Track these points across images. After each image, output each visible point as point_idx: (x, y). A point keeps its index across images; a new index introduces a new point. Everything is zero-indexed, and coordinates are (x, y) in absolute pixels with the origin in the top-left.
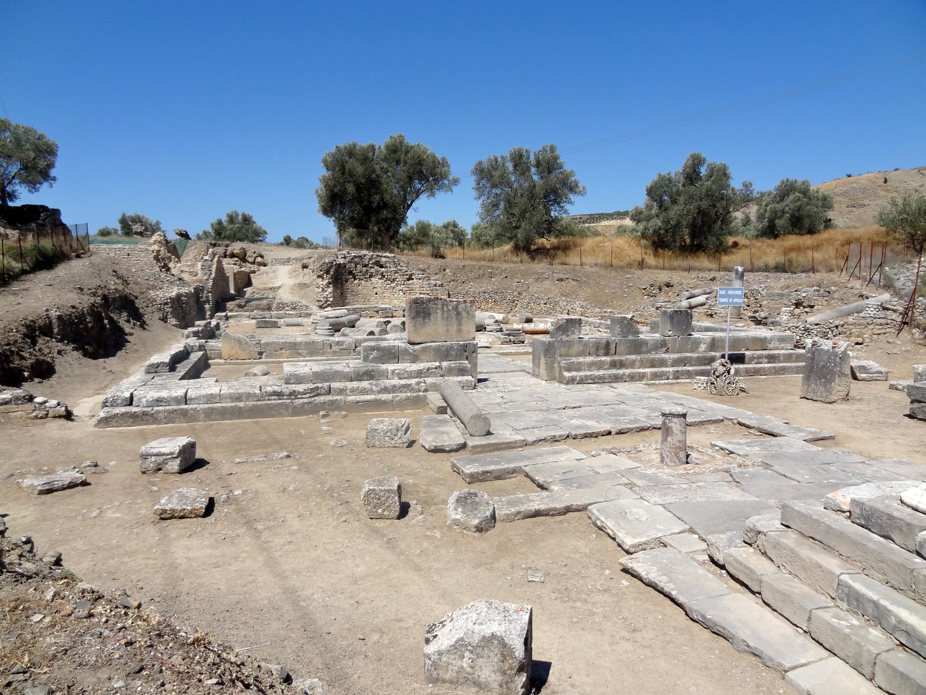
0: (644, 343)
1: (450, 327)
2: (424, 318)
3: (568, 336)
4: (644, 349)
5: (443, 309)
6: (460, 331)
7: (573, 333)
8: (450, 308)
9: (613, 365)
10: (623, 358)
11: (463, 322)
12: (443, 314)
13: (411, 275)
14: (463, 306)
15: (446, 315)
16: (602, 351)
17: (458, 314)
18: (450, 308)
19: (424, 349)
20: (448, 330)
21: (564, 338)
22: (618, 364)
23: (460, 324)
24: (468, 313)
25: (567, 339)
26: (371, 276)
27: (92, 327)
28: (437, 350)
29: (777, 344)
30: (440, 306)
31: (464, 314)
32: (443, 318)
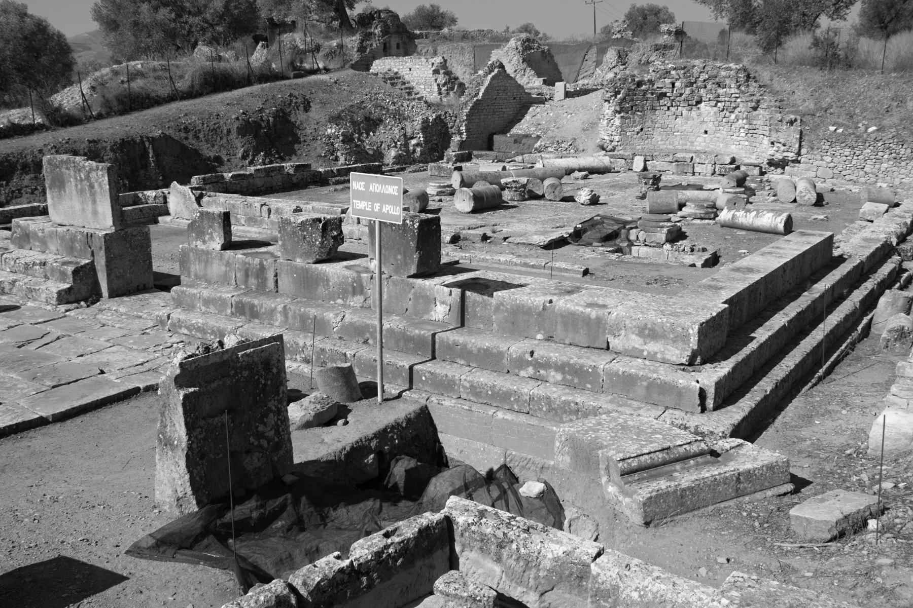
0: (325, 279)
3: (204, 242)
4: (321, 290)
6: (95, 213)
7: (212, 239)
8: (83, 176)
12: (76, 186)
13: (758, 101)
15: (79, 186)
17: (91, 187)
18: (83, 176)
20: (83, 210)
23: (94, 202)
24: (100, 185)
25: (203, 247)
26: (698, 102)
28: (62, 239)
29: (635, 341)
30: (72, 173)
31: (96, 185)
32: (77, 190)
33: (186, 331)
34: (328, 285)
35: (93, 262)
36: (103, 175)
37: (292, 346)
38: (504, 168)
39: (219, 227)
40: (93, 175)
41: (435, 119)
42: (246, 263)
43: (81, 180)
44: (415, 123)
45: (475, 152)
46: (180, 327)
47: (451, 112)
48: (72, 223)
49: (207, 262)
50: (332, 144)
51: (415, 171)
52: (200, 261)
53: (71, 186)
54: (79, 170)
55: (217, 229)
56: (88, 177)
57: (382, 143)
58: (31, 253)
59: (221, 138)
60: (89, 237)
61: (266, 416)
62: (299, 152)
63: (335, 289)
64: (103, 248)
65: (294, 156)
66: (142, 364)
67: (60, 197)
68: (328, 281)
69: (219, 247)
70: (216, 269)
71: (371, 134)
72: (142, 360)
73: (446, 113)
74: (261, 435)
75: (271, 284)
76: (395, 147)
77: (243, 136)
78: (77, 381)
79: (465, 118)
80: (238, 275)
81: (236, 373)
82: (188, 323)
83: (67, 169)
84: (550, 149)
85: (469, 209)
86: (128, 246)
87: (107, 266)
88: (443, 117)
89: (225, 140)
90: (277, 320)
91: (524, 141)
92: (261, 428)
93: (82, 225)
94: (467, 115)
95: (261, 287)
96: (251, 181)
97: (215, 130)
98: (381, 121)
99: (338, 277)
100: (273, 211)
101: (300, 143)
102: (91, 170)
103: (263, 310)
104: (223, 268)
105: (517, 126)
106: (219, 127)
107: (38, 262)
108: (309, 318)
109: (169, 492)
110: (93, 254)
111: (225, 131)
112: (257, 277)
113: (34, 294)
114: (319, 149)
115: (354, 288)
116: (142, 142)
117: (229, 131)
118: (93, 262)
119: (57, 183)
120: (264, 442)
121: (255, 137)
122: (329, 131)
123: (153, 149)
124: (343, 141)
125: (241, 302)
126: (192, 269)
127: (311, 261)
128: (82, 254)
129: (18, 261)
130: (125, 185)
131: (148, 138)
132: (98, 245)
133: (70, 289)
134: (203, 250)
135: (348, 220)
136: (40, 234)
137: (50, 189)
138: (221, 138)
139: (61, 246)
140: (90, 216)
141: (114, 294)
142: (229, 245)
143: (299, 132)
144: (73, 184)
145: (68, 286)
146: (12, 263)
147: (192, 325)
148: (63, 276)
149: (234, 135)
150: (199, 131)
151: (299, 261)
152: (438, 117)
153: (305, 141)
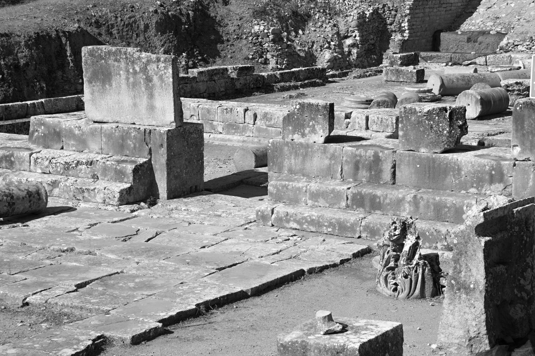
0: (458, 169)
1: (138, 100)
2: (104, 83)
3: (303, 135)
4: (451, 180)
5: (128, 71)
6: (151, 108)
9: (358, 201)
10: (379, 192)
11: (156, 93)
12: (127, 79)
14: (154, 66)
15: (131, 80)
16: (364, 174)
17: (149, 80)
18: (137, 69)
19: (93, 133)
20: (135, 105)
21: (297, 138)
22: (367, 203)
23: (151, 96)
24: (161, 78)
25: (302, 140)
27: (27, 65)
28: (109, 136)
30: (123, 65)
31: (155, 79)
32: (128, 84)
33: (295, 226)
34: (459, 174)
35: (150, 160)
36: (165, 68)
37: (432, 234)
38: (476, 71)
39: (324, 119)
40: (152, 67)
41: (372, 14)
42: (356, 155)
43: (135, 73)
44: (350, 19)
45: (423, 54)
46: (288, 221)
47: (390, 5)
48: (118, 119)
49: (305, 156)
50: (261, 44)
51: (360, 77)
52: (296, 155)
53: (120, 80)
54: (133, 62)
55: (321, 121)
56: (144, 70)
57: (313, 43)
58: (65, 152)
59: (138, 35)
60: (147, 134)
61: (525, 270)
62: (223, 54)
63: (468, 178)
64: (165, 145)
65: (217, 59)
66: (277, 253)
67: (103, 91)
68: (459, 170)
69: (322, 140)
70: (318, 162)
71: (300, 32)
72: (275, 250)
73: (384, 6)
74: (521, 288)
75: (387, 176)
76: (329, 48)
77: (163, 33)
78: (243, 262)
79: (408, 12)
80: (345, 168)
81: (511, 228)
82: (299, 217)
83: (116, 60)
84: (520, 48)
85: (475, 116)
86: (185, 144)
87: (168, 164)
88: (380, 11)
89: (142, 38)
90: (404, 210)
91: (480, 39)
92: (522, 282)
93: (130, 122)
94: (410, 9)
95: (375, 178)
96: (194, 85)
97: (131, 26)
98: (309, 16)
99: (473, 166)
100: (259, 117)
101: (222, 42)
102: (149, 61)
103: (388, 201)
104: (327, 162)
105: (468, 21)
106: (135, 22)
107: (84, 161)
108: (446, 207)
109: (461, 333)
110: (150, 153)
111: (142, 27)
112: (370, 169)
113: (86, 194)
114: (245, 50)
115: (491, 176)
116: (58, 37)
117: (147, 27)
118: (150, 160)
119: (101, 77)
120: (524, 294)
121: (175, 34)
122: (256, 28)
123: (70, 46)
124: (274, 41)
125: (360, 193)
126: (286, 163)
127: (439, 151)
128: (137, 151)
129: (54, 161)
130: (42, 88)
131: (64, 32)
132: (159, 142)
133: (130, 188)
134: (301, 144)
135: (353, 126)
136: (77, 132)
137: (90, 82)
138: (138, 35)
139: (106, 143)
140: (144, 111)
141: (173, 195)
142: (329, 140)
143: (221, 30)
144: (123, 77)
145: (128, 185)
146: (47, 163)
147: (305, 218)
148: (119, 175)
149: (152, 31)
150: (112, 25)
151: (423, 151)
152: (376, 11)
153: (228, 40)
